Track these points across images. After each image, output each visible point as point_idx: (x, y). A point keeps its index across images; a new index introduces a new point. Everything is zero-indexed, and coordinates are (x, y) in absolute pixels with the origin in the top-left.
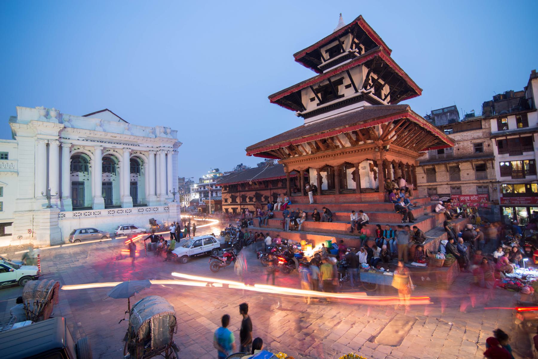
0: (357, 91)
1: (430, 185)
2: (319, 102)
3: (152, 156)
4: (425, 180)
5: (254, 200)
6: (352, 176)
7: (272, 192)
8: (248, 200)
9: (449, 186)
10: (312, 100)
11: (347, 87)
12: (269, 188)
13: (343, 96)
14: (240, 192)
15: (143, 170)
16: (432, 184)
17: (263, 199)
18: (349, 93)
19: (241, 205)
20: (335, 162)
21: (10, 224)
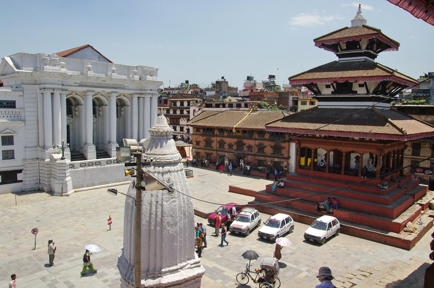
0: (368, 92)
1: (414, 158)
2: (333, 91)
3: (135, 100)
4: (410, 153)
5: (235, 147)
6: (355, 160)
7: (257, 142)
8: (226, 146)
9: (430, 161)
10: (328, 86)
11: (361, 86)
12: (254, 137)
13: (356, 92)
14: (217, 136)
15: (122, 113)
16: (416, 157)
17: (245, 149)
18: (362, 91)
19: (217, 150)
20: (344, 149)
21: (20, 171)
